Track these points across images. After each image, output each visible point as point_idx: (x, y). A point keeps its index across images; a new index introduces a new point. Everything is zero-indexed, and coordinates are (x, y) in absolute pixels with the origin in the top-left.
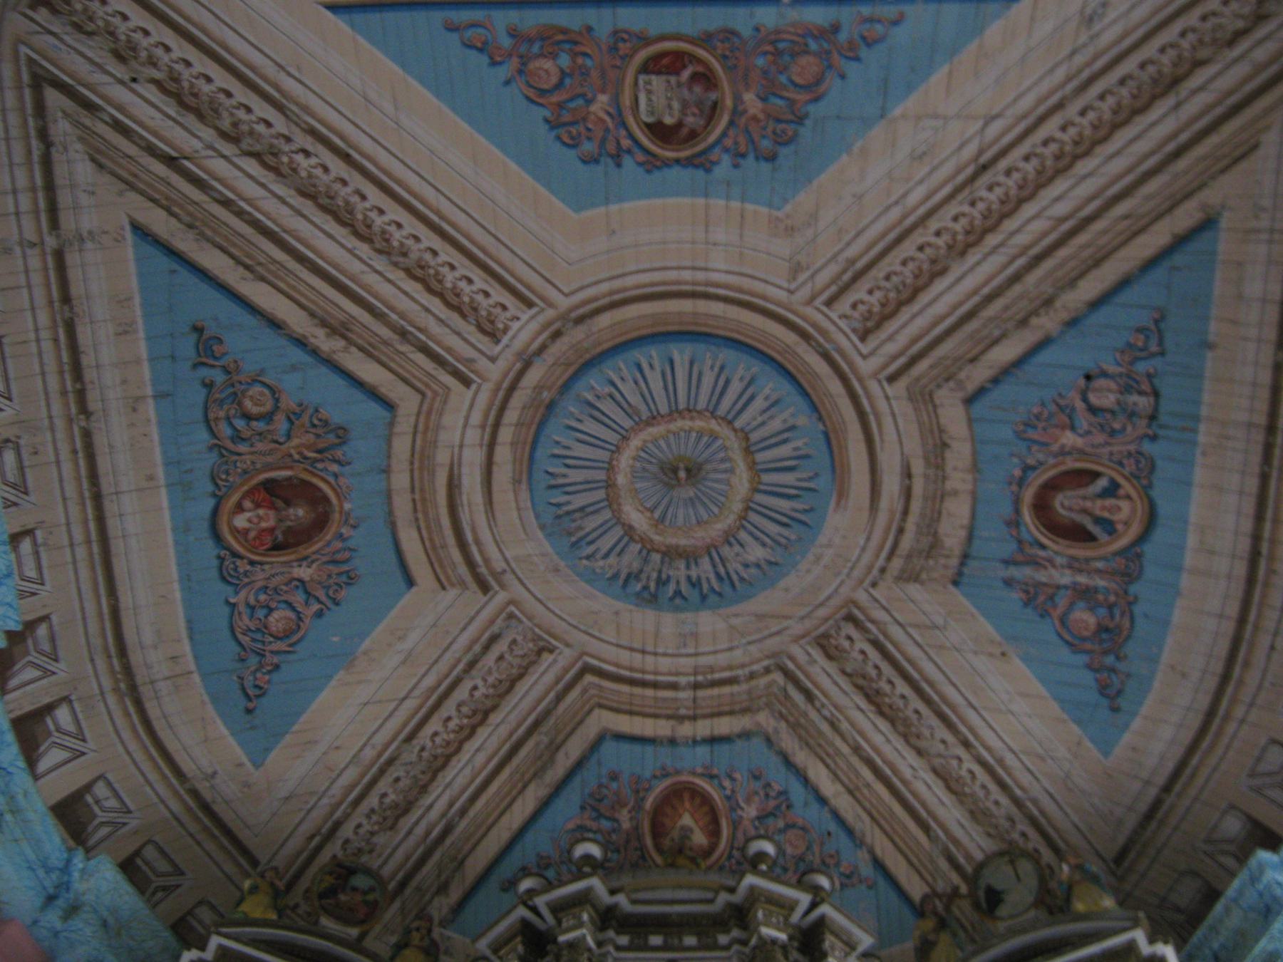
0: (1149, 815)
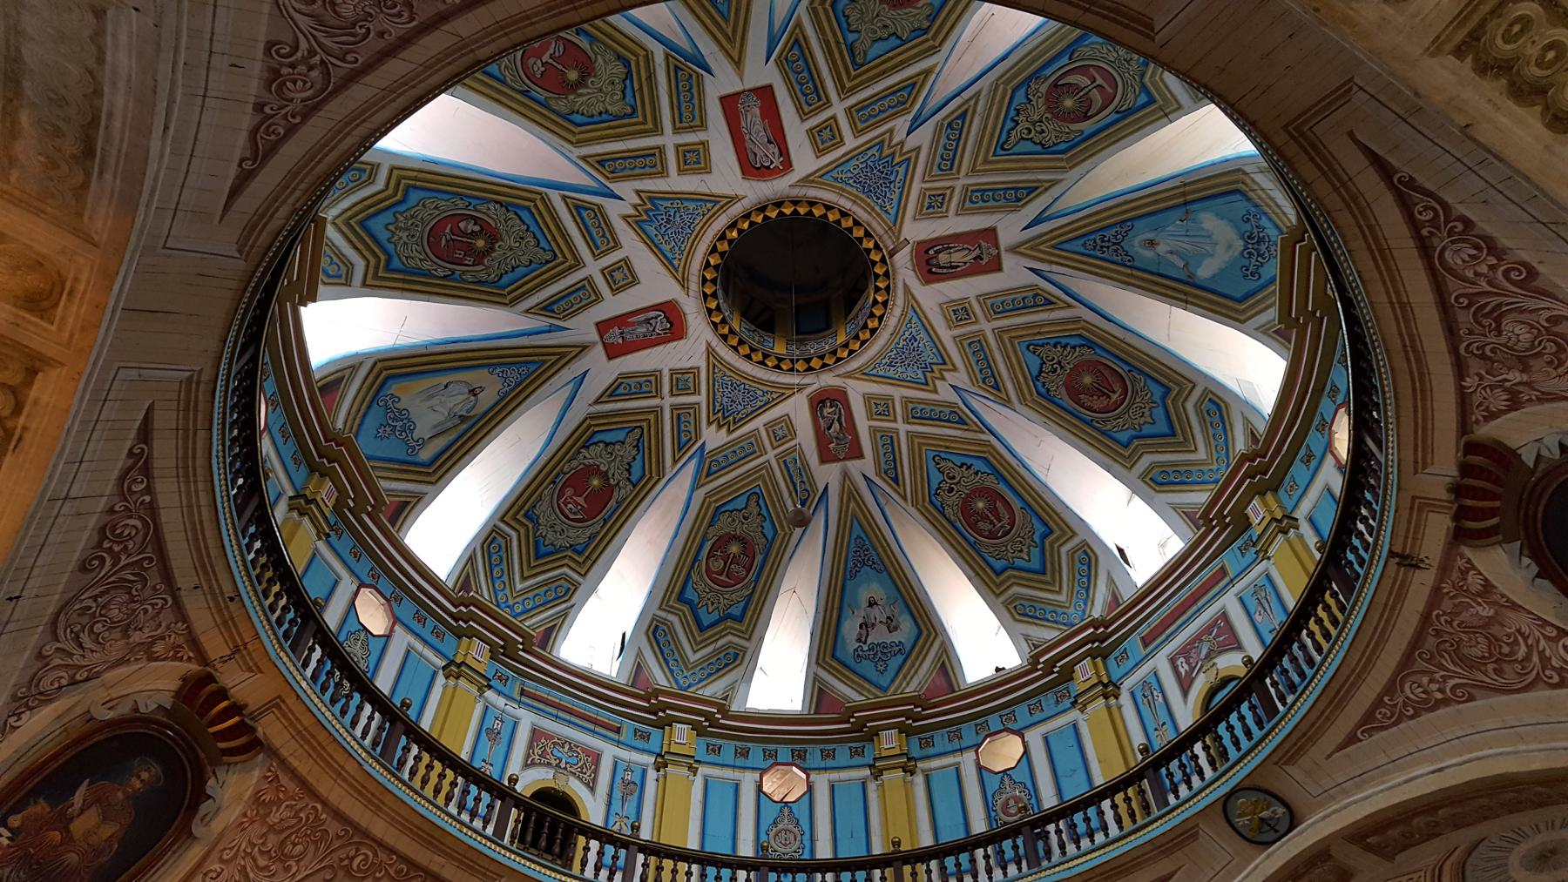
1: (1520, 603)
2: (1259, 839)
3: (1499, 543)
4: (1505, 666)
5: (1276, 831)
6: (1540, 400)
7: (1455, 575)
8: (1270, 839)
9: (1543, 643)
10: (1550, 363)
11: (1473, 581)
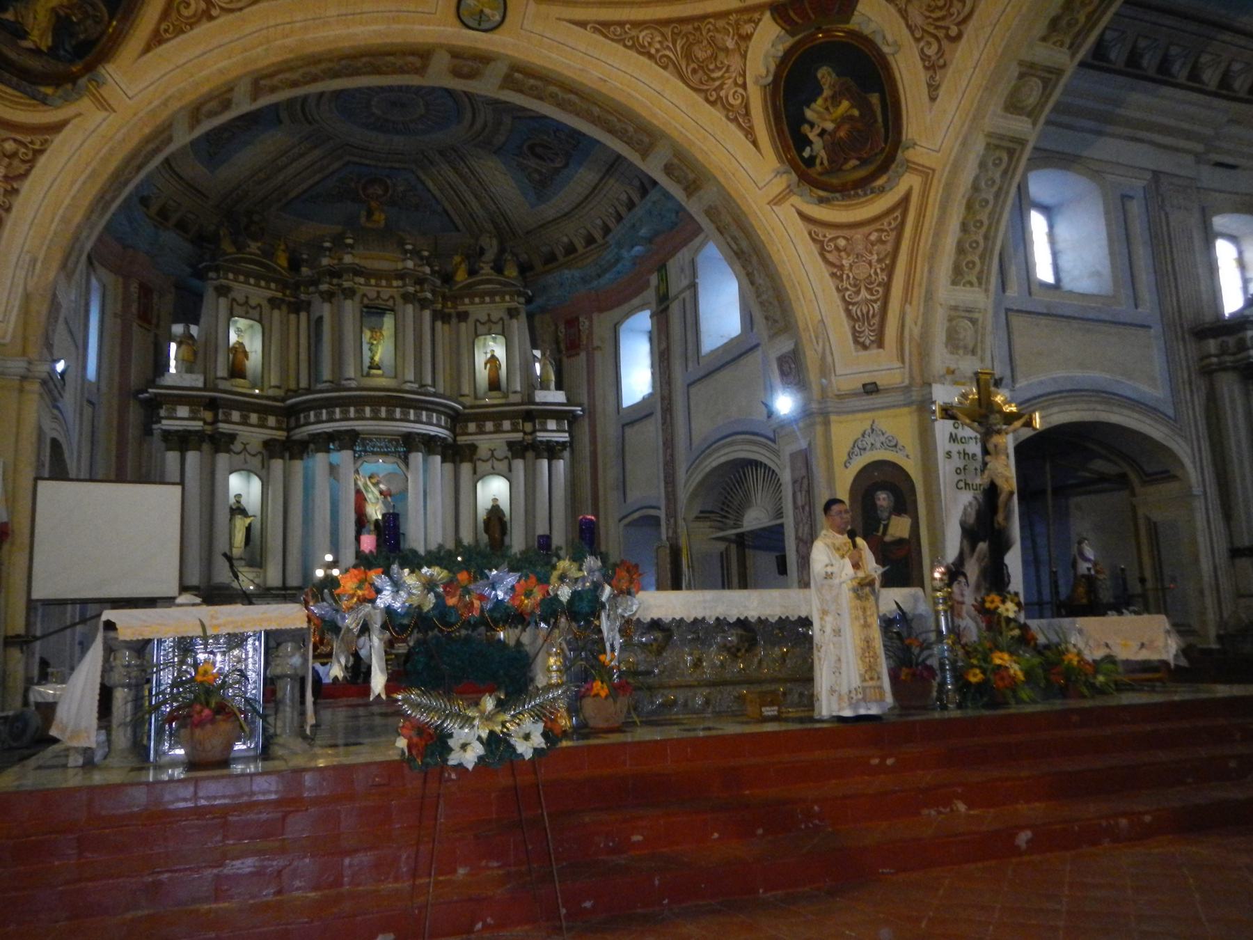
0: (541, 226)
1: (749, 56)
2: (465, 19)
3: (783, 28)
4: (701, 72)
5: (479, 24)
6: (900, 11)
7: (746, 17)
8: (471, 24)
9: (730, 81)
10: (929, 6)
11: (748, 28)
